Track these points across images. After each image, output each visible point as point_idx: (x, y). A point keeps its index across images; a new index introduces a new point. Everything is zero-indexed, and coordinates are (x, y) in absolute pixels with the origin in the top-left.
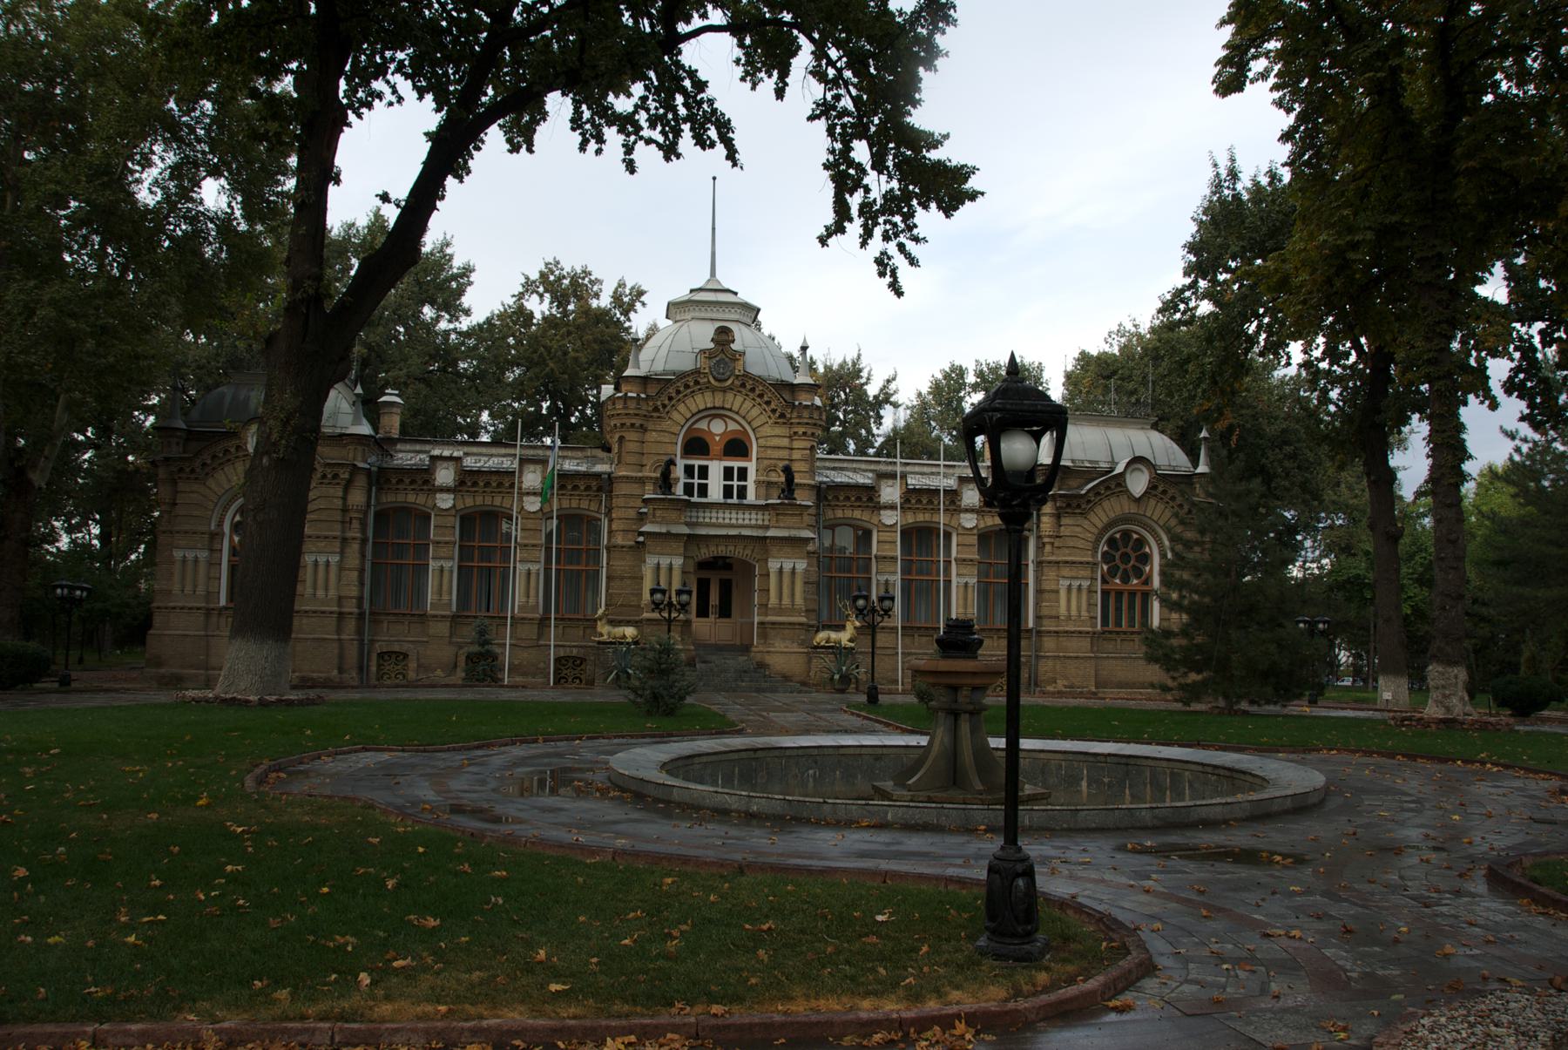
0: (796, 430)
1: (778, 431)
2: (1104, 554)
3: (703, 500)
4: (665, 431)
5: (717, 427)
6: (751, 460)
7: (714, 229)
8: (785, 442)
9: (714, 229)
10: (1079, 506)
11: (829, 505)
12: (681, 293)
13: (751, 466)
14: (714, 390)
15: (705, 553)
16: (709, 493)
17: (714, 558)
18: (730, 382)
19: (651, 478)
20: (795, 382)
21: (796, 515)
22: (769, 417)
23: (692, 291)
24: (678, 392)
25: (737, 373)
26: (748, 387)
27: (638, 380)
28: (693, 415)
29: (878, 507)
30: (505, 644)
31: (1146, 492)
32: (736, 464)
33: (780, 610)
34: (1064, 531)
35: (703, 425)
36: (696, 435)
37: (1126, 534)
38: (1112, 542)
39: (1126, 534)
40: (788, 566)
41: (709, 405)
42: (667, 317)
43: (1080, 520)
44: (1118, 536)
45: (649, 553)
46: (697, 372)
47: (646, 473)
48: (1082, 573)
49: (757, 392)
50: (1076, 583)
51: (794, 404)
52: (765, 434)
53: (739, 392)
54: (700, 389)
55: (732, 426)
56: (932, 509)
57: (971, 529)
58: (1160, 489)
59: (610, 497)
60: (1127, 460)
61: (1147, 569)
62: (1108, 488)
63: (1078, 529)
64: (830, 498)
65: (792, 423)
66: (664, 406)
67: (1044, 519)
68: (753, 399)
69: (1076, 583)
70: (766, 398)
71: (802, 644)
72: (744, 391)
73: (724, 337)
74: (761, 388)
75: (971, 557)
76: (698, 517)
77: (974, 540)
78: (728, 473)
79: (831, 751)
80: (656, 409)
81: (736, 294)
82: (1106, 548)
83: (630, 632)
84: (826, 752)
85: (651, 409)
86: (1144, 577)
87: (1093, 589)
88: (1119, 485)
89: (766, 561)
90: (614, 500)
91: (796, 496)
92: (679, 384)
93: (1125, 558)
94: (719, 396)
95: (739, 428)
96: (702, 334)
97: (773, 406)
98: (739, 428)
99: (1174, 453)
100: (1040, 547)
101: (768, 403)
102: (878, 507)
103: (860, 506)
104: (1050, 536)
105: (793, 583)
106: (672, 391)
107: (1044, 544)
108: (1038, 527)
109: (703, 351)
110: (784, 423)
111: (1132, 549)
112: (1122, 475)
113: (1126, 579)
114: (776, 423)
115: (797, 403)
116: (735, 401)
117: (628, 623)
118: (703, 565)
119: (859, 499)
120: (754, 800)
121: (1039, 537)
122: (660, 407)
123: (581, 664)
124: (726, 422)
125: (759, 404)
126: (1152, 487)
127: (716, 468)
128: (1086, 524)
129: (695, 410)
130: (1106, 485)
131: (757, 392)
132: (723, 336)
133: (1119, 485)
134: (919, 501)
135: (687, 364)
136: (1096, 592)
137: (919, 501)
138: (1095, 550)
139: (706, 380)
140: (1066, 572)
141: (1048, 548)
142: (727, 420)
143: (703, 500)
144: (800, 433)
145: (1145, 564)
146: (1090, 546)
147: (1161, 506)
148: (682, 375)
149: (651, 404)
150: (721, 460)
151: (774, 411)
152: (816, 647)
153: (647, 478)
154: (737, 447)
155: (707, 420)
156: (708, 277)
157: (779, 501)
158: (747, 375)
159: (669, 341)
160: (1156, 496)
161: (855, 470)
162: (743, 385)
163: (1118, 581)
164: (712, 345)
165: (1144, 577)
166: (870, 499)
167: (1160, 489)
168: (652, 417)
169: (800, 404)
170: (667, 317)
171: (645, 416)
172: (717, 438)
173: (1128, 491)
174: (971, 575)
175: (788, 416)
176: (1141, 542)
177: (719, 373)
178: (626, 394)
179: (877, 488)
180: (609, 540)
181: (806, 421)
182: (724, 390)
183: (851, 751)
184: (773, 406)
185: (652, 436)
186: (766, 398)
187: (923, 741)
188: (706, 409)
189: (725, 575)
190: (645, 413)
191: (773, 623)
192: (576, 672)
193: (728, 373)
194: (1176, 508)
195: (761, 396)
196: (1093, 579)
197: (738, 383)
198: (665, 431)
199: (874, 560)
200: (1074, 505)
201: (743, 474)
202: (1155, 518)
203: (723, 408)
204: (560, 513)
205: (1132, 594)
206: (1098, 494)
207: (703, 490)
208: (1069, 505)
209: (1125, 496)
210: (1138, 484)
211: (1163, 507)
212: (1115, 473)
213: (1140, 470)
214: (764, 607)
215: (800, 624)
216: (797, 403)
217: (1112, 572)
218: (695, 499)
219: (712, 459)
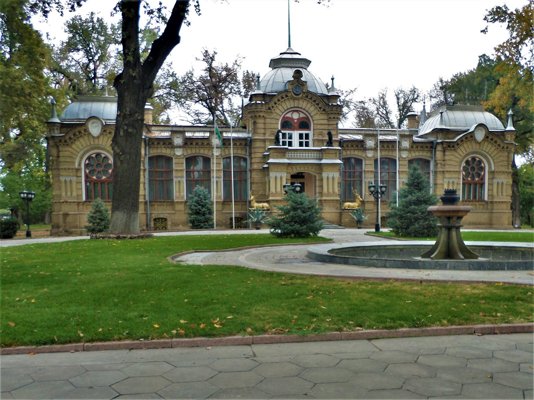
0: (330, 116)
1: (322, 117)
2: (464, 167)
3: (290, 148)
4: (273, 118)
5: (296, 116)
6: (310, 130)
7: (289, 24)
8: (325, 122)
9: (289, 24)
10: (453, 147)
11: (344, 149)
12: (277, 56)
13: (311, 133)
14: (294, 99)
15: (295, 171)
16: (293, 145)
17: (298, 173)
18: (301, 95)
19: (269, 139)
20: (329, 95)
21: (333, 153)
22: (318, 111)
23: (281, 54)
24: (279, 100)
25: (304, 91)
26: (309, 97)
27: (261, 96)
28: (285, 111)
29: (365, 149)
30: (232, 213)
31: (483, 140)
32: (304, 132)
33: (328, 194)
34: (447, 158)
35: (289, 115)
36: (286, 120)
37: (474, 159)
38: (467, 162)
39: (474, 159)
40: (331, 176)
41: (292, 106)
42: (269, 67)
43: (453, 153)
44: (470, 159)
45: (272, 171)
46: (286, 91)
47: (267, 137)
48: (454, 176)
49: (313, 99)
50: (451, 181)
51: (329, 104)
52: (317, 119)
53: (305, 100)
54: (288, 99)
55: (302, 115)
56: (389, 150)
57: (405, 158)
58: (490, 138)
59: (250, 147)
60: (476, 125)
61: (483, 173)
62: (467, 138)
63: (452, 157)
64: (345, 146)
65: (328, 114)
66: (273, 107)
67: (438, 153)
68: (311, 103)
69: (451, 181)
70: (317, 102)
71: (337, 209)
72: (307, 99)
73: (298, 75)
74: (315, 98)
75: (405, 170)
76: (297, 156)
77: (406, 163)
78: (301, 136)
79: (383, 247)
80: (269, 109)
81: (300, 54)
82: (464, 165)
83: (266, 205)
84: (381, 248)
85: (267, 108)
86: (481, 177)
87: (459, 182)
88: (472, 137)
89: (321, 174)
90: (252, 150)
91: (333, 145)
92: (279, 97)
93: (473, 168)
94: (296, 102)
95: (305, 116)
96: (288, 74)
97: (320, 106)
98: (305, 116)
99: (496, 122)
100: (436, 165)
101: (318, 104)
102: (365, 149)
103: (357, 149)
104: (440, 160)
105: (333, 183)
106: (276, 100)
107: (437, 164)
108: (435, 156)
109: (289, 81)
110: (325, 113)
111: (476, 165)
112: (473, 132)
113: (473, 178)
114: (322, 113)
115: (330, 104)
116: (304, 104)
117: (264, 202)
118: (293, 176)
119: (352, 146)
120: (388, 261)
121: (435, 161)
122: (271, 107)
123: (241, 220)
124: (299, 114)
125: (314, 105)
126: (487, 137)
127: (296, 134)
128: (456, 154)
129: (286, 108)
130: (466, 136)
131: (313, 99)
132: (298, 74)
133: (472, 137)
134: (388, 147)
135: (281, 88)
136: (460, 184)
137: (388, 147)
138: (460, 165)
139: (291, 95)
140: (447, 175)
141: (439, 166)
142: (300, 112)
143: (290, 148)
144: (332, 117)
145: (482, 171)
146: (458, 164)
147: (490, 146)
148: (280, 93)
149: (267, 106)
150: (298, 130)
151: (320, 108)
152: (344, 210)
153: (267, 139)
154: (304, 124)
155: (291, 112)
156: (288, 47)
157: (326, 148)
158: (309, 92)
159: (273, 77)
160: (488, 141)
161: (352, 134)
162: (307, 97)
163: (469, 179)
164: (293, 79)
165: (481, 177)
166: (362, 146)
167: (490, 138)
168: (267, 112)
169: (332, 104)
170: (269, 67)
171: (265, 112)
172: (296, 121)
173: (475, 139)
174: (371, 178)
175: (327, 110)
176: (480, 162)
177: (297, 92)
178: (256, 102)
179: (365, 141)
180: (251, 167)
181: (334, 112)
182: (298, 99)
183: (391, 247)
184: (320, 106)
185: (268, 121)
186: (317, 102)
187: (433, 242)
188: (291, 108)
189: (301, 180)
190: (265, 110)
191: (325, 200)
192: (239, 224)
193: (301, 92)
194: (497, 147)
195: (315, 101)
196: (459, 178)
197: (304, 95)
198: (273, 118)
199: (363, 173)
200: (451, 146)
201: (307, 136)
202: (487, 151)
203: (298, 107)
204: (235, 155)
205: (475, 184)
206: (462, 141)
207: (290, 144)
208: (449, 146)
209: (474, 142)
210: (480, 136)
211: (491, 146)
212: (469, 131)
213: (482, 130)
214: (321, 193)
215: (337, 200)
216: (330, 104)
217: (467, 175)
218: (304, 148)
219: (294, 130)
